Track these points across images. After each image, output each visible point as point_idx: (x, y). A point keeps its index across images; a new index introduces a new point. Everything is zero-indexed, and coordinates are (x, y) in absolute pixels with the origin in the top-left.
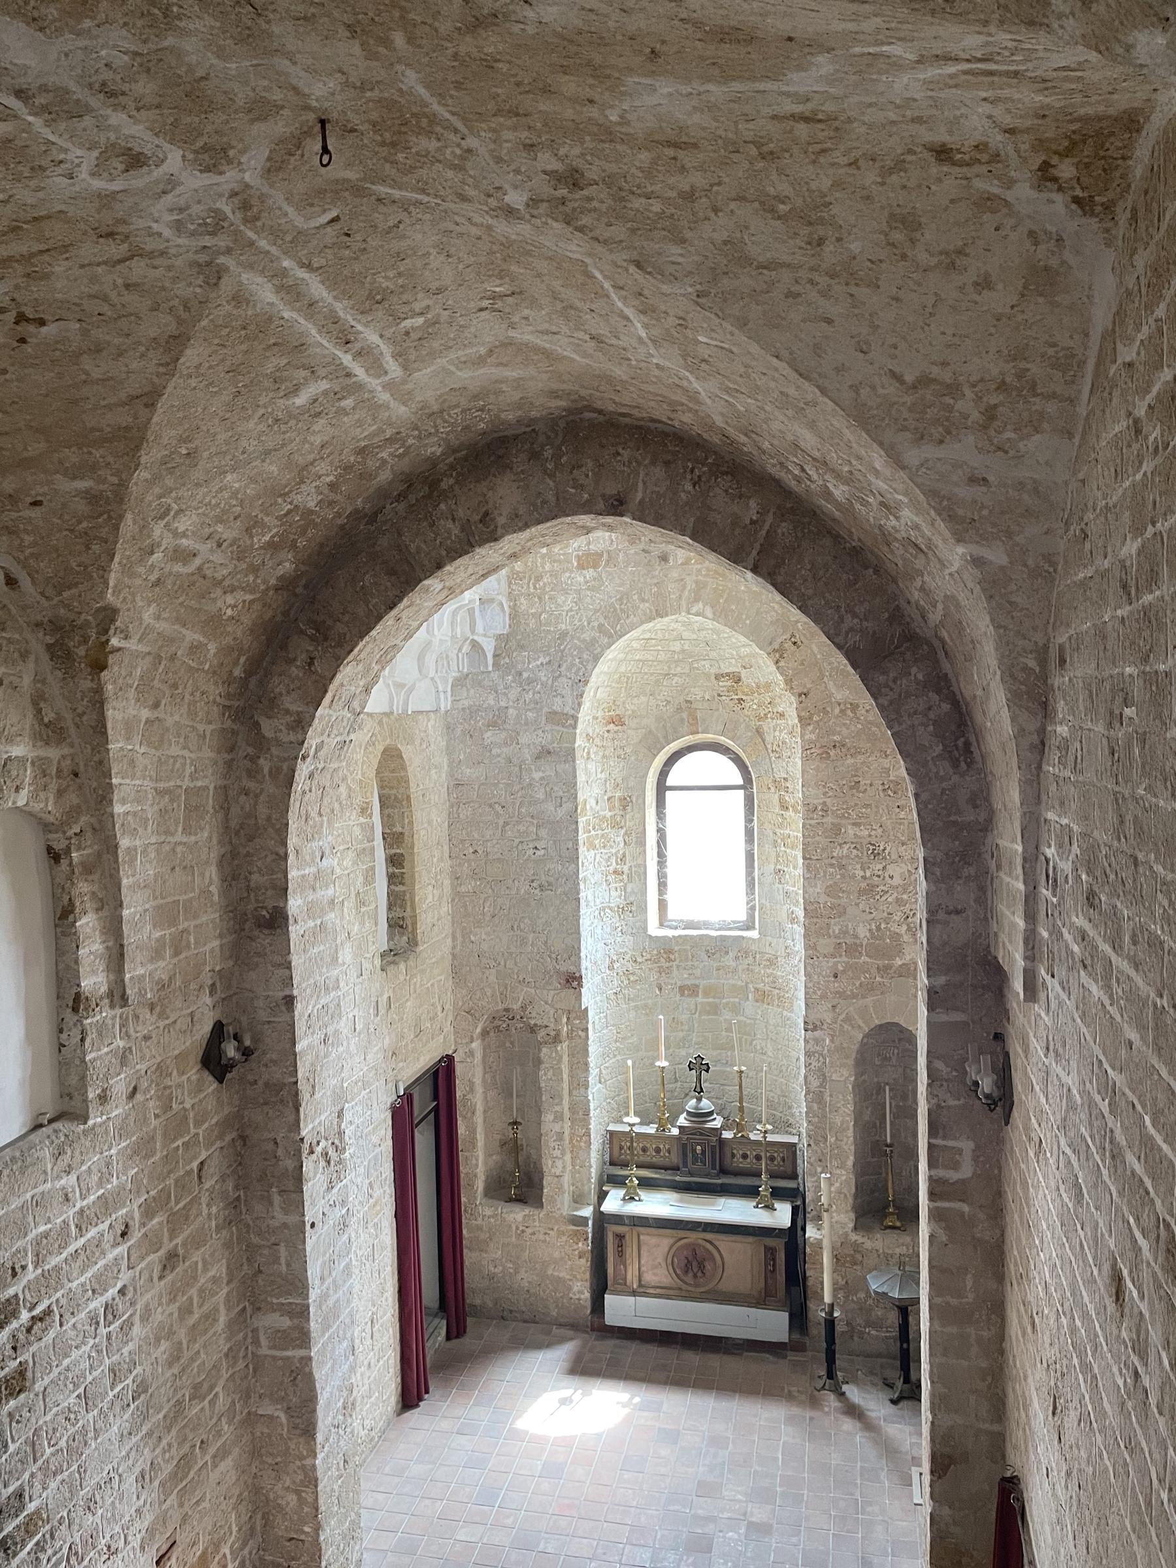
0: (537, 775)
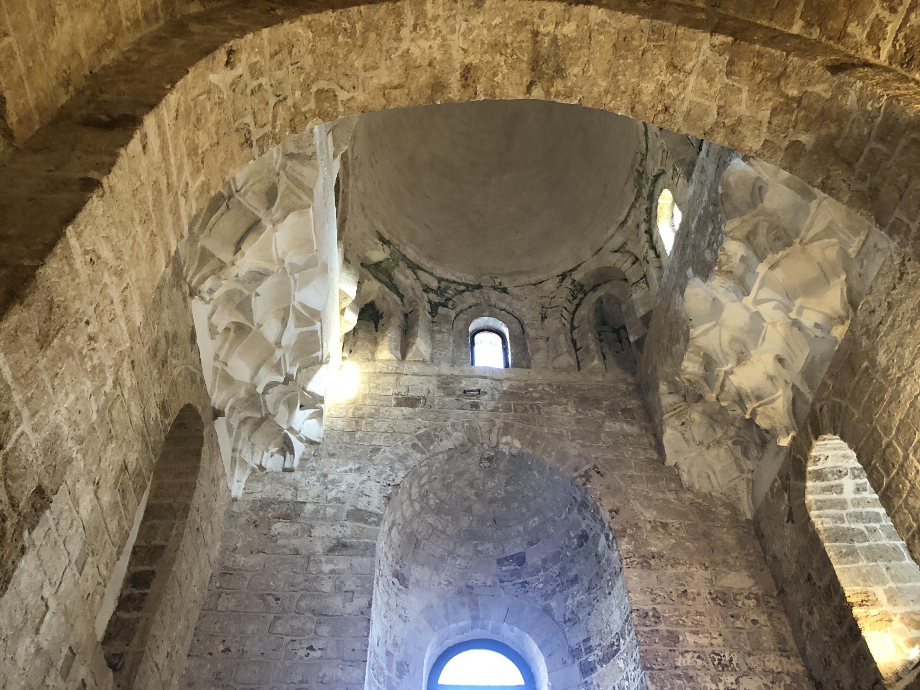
0: (327, 568)
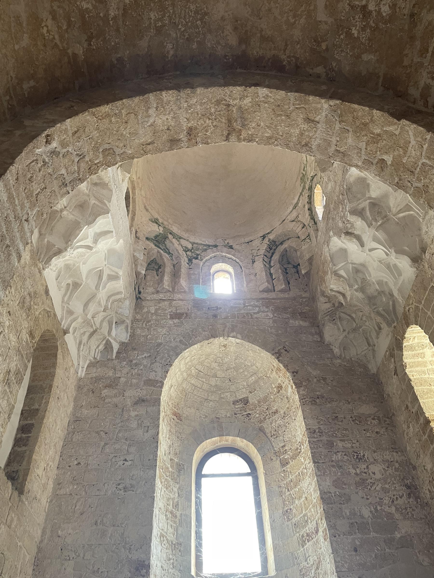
0: (133, 414)
